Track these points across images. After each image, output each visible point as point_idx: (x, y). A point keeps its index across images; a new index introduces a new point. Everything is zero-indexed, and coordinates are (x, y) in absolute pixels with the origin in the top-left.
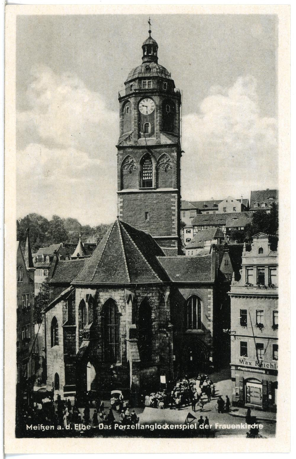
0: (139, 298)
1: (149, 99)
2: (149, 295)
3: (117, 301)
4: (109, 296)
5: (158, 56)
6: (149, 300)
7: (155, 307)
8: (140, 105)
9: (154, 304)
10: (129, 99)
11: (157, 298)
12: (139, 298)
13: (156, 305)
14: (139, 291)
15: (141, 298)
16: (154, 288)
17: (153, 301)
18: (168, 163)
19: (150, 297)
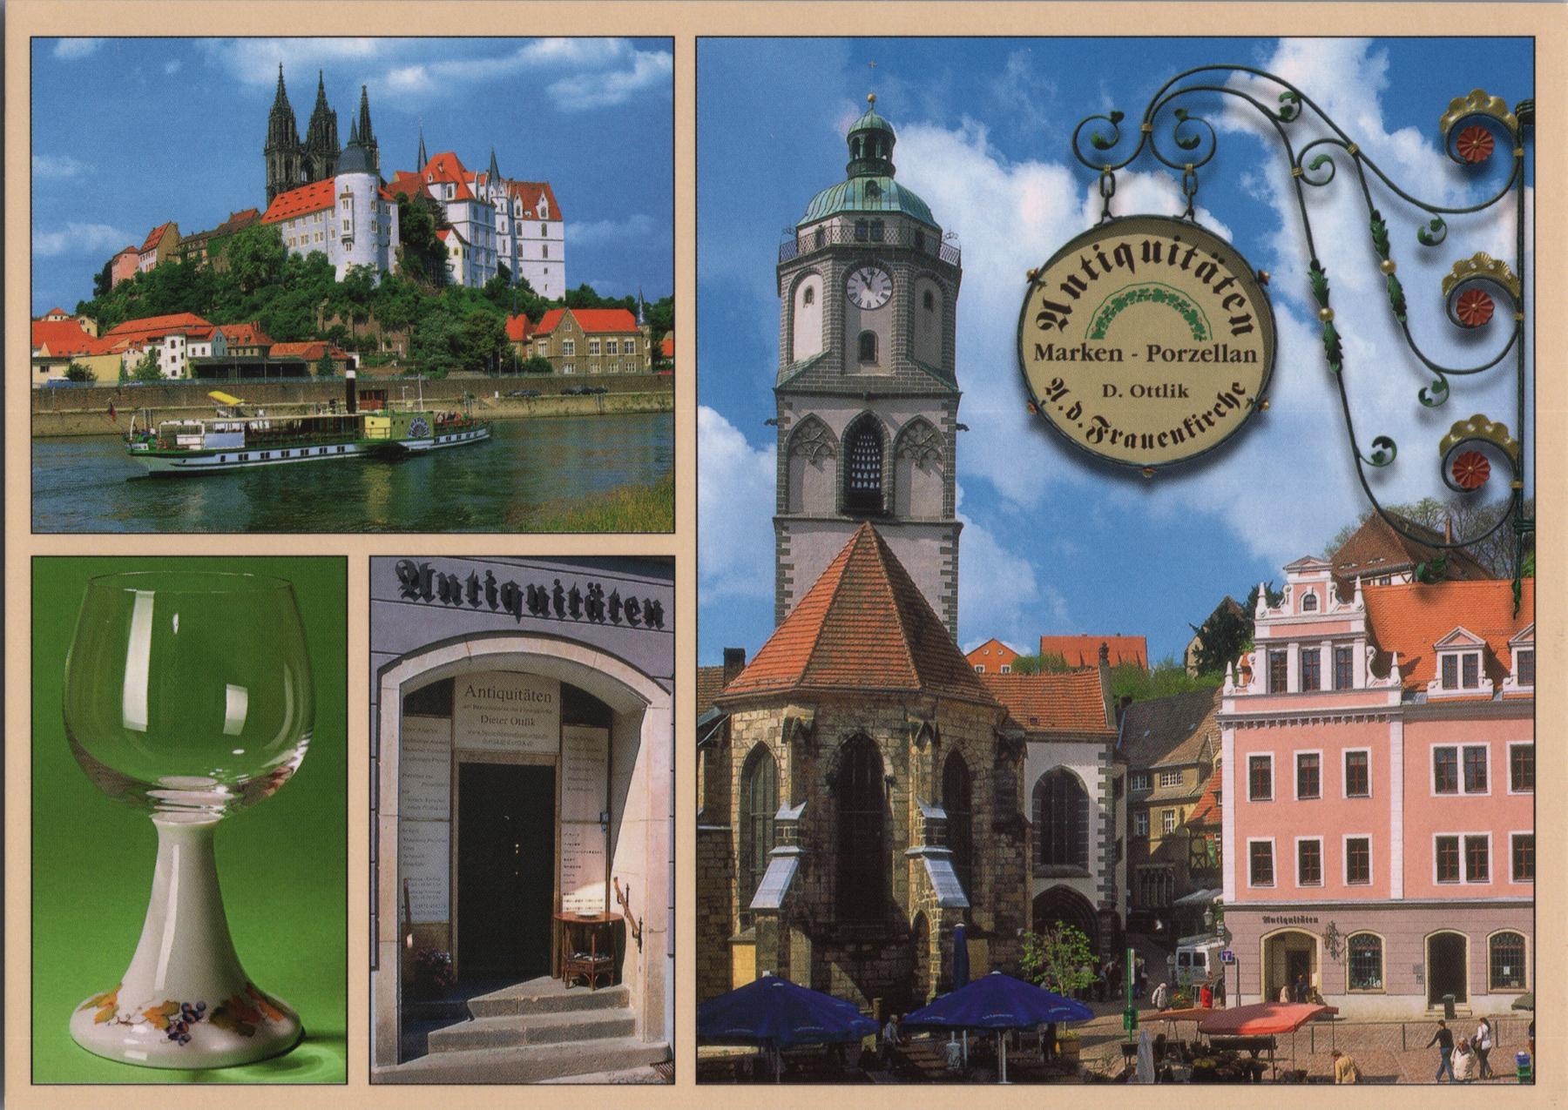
5: (894, 162)
6: (969, 751)
8: (851, 283)
10: (818, 267)
11: (989, 746)
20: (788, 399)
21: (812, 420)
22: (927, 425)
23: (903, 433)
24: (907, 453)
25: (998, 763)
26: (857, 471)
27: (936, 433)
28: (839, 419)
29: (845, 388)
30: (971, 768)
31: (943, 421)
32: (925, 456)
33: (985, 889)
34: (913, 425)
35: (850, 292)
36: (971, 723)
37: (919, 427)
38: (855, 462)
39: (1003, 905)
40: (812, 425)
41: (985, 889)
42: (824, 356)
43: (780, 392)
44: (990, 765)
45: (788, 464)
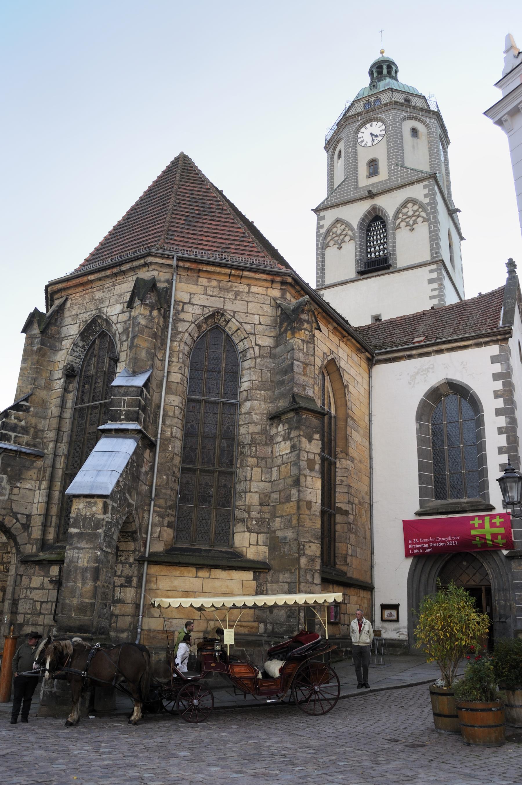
0: (189, 308)
1: (374, 123)
2: (229, 306)
3: (114, 319)
4: (94, 312)
6: (233, 325)
7: (257, 348)
9: (252, 337)
12: (189, 308)
13: (259, 342)
14: (193, 288)
15: (199, 312)
16: (254, 289)
17: (248, 327)
18: (417, 214)
19: (235, 312)
20: (322, 214)
21: (338, 221)
22: (414, 201)
23: (398, 212)
24: (403, 224)
25: (279, 339)
26: (370, 247)
27: (421, 206)
28: (355, 214)
29: (357, 196)
30: (241, 347)
31: (425, 196)
32: (415, 222)
33: (252, 499)
34: (404, 205)
35: (359, 140)
36: (237, 294)
37: (410, 205)
38: (370, 241)
39: (277, 523)
40: (339, 225)
41: (252, 499)
42: (344, 181)
43: (317, 211)
44: (267, 342)
45: (323, 254)
